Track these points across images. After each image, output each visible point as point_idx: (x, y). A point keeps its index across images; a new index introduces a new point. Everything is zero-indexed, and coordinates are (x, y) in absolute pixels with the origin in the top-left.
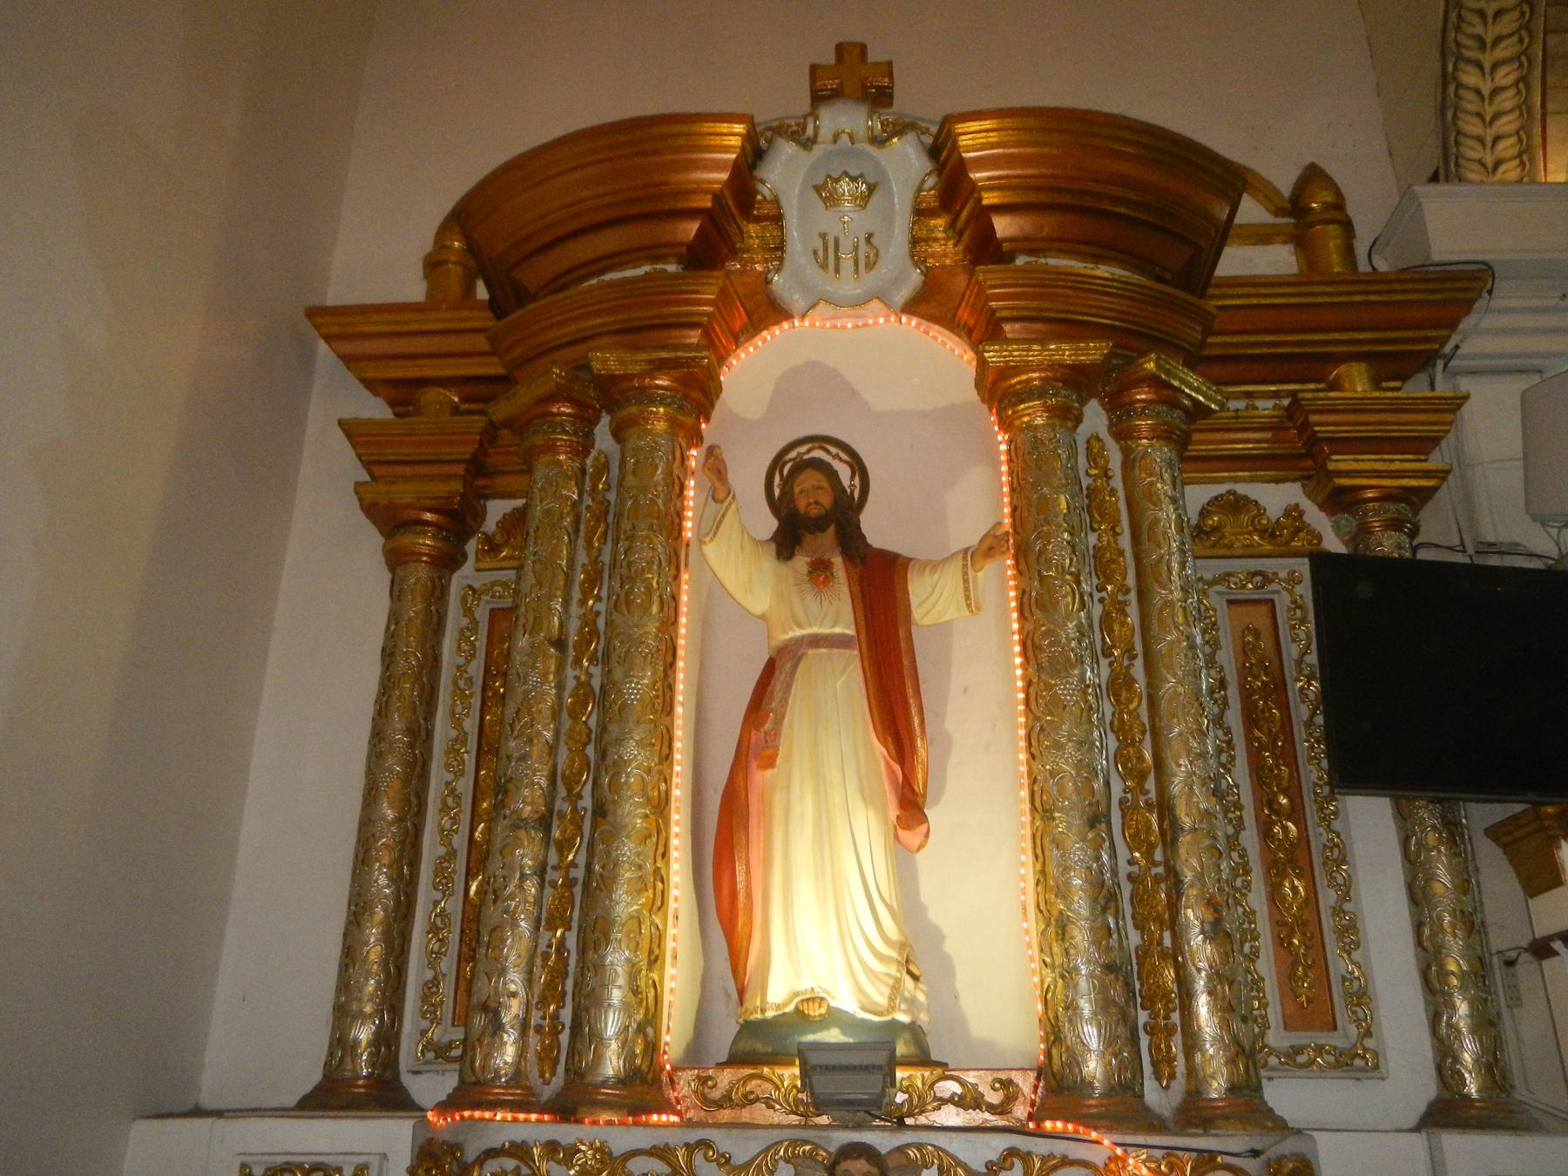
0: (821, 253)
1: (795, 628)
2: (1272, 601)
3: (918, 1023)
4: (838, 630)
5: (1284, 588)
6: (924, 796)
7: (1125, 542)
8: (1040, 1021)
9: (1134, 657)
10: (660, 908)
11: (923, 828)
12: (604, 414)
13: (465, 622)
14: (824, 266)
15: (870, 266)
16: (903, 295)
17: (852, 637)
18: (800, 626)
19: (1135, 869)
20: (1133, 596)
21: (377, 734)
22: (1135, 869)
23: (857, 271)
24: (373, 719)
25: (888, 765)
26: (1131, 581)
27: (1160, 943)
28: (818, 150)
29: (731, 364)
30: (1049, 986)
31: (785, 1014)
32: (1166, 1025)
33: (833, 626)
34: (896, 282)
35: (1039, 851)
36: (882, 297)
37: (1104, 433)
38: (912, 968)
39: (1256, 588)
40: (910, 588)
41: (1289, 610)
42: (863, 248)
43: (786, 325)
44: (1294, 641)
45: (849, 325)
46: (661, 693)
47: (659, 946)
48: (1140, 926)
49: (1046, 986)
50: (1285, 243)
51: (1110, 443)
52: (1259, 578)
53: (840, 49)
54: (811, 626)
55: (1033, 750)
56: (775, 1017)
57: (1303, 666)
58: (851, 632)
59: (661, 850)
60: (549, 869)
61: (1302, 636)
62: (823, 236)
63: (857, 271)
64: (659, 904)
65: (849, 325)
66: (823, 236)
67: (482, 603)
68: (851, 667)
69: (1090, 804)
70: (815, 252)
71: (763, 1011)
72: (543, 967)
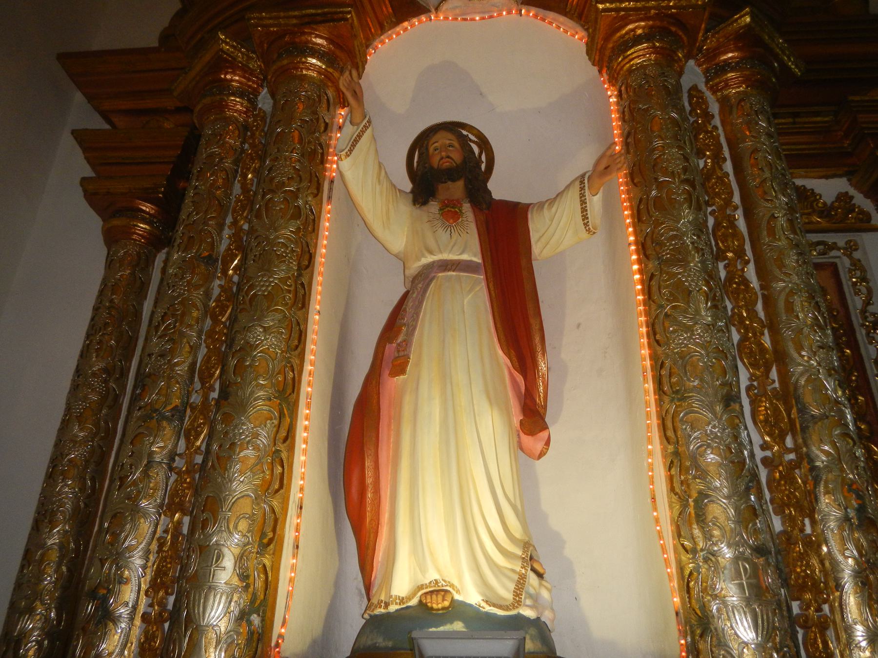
1: (427, 254)
3: (543, 619)
4: (465, 257)
5: (844, 254)
6: (545, 407)
7: (728, 167)
8: (677, 614)
10: (277, 491)
17: (478, 263)
18: (431, 253)
19: (768, 453)
22: (768, 453)
25: (511, 375)
27: (802, 530)
29: (377, 47)
30: (691, 574)
31: (408, 607)
32: (819, 617)
33: (460, 254)
35: (670, 433)
38: (536, 566)
39: (819, 254)
40: (531, 226)
41: (850, 271)
43: (423, 18)
44: (856, 294)
45: (477, 18)
46: (292, 289)
47: (274, 530)
48: (780, 511)
49: (687, 572)
51: (708, 94)
52: (821, 247)
54: (441, 252)
55: (658, 337)
56: (397, 611)
57: (867, 314)
58: (478, 259)
59: (283, 433)
61: (864, 290)
64: (276, 487)
65: (477, 18)
69: (723, 385)
71: (387, 605)
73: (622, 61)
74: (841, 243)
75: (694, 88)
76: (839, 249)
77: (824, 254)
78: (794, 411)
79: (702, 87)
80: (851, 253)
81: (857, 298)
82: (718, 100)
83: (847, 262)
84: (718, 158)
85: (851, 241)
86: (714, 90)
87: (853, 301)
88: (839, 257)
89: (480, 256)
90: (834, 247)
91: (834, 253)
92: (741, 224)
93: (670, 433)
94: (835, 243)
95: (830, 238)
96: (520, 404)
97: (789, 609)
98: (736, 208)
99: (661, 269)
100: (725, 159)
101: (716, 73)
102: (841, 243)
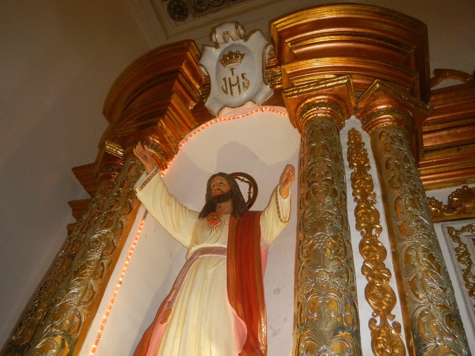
0: (224, 87)
4: (218, 245)
14: (226, 92)
16: (261, 98)
17: (224, 248)
25: (236, 320)
29: (188, 138)
36: (252, 99)
37: (359, 128)
40: (261, 223)
43: (213, 121)
45: (240, 117)
62: (225, 79)
65: (240, 117)
66: (225, 79)
68: (221, 263)
73: (302, 120)
78: (412, 340)
89: (227, 244)
96: (241, 341)
99: (304, 237)
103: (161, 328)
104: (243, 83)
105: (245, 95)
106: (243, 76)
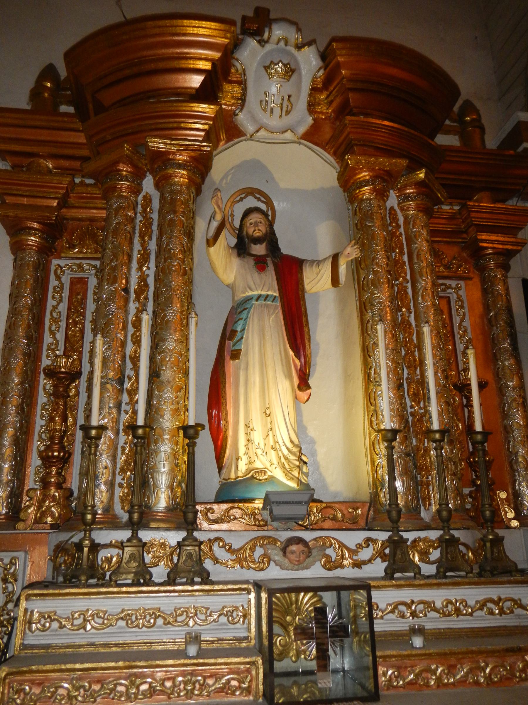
2: (449, 297)
5: (454, 292)
7: (406, 258)
9: (411, 313)
11: (308, 391)
12: (148, 174)
13: (56, 283)
15: (288, 113)
16: (302, 130)
19: (413, 410)
20: (409, 285)
21: (9, 338)
22: (413, 410)
23: (281, 116)
24: (6, 330)
26: (408, 277)
27: (424, 444)
28: (268, 47)
30: (378, 464)
32: (427, 481)
34: (299, 123)
37: (396, 207)
38: (304, 458)
39: (442, 291)
41: (456, 301)
42: (286, 103)
44: (458, 315)
46: (186, 317)
48: (416, 437)
49: (376, 464)
50: (455, 135)
51: (398, 211)
52: (443, 287)
53: (257, 10)
57: (462, 327)
60: (123, 404)
61: (462, 313)
63: (281, 116)
67: (66, 274)
69: (397, 379)
70: (261, 102)
72: (122, 454)
74: (454, 285)
75: (392, 208)
76: (452, 289)
77: (445, 291)
79: (396, 207)
80: (458, 291)
81: (458, 317)
82: (403, 215)
83: (455, 296)
84: (402, 253)
85: (458, 284)
86: (402, 209)
87: (456, 319)
88: (451, 293)
90: (450, 287)
91: (450, 291)
92: (410, 291)
93: (372, 401)
94: (450, 285)
95: (448, 282)
97: (416, 478)
98: (408, 282)
100: (404, 254)
101: (404, 200)
102: (454, 285)
103: (231, 365)
104: (288, 106)
105: (287, 120)
106: (290, 96)
